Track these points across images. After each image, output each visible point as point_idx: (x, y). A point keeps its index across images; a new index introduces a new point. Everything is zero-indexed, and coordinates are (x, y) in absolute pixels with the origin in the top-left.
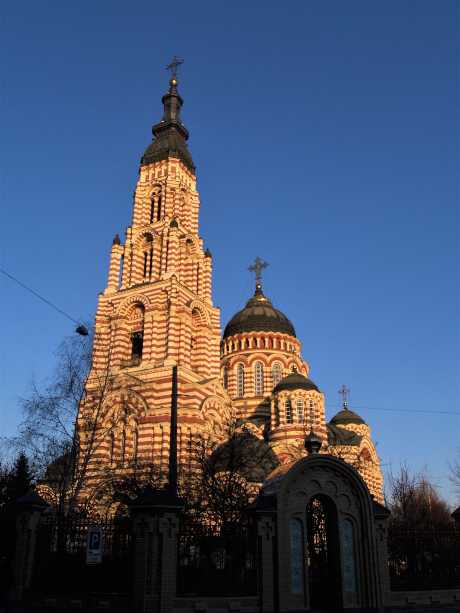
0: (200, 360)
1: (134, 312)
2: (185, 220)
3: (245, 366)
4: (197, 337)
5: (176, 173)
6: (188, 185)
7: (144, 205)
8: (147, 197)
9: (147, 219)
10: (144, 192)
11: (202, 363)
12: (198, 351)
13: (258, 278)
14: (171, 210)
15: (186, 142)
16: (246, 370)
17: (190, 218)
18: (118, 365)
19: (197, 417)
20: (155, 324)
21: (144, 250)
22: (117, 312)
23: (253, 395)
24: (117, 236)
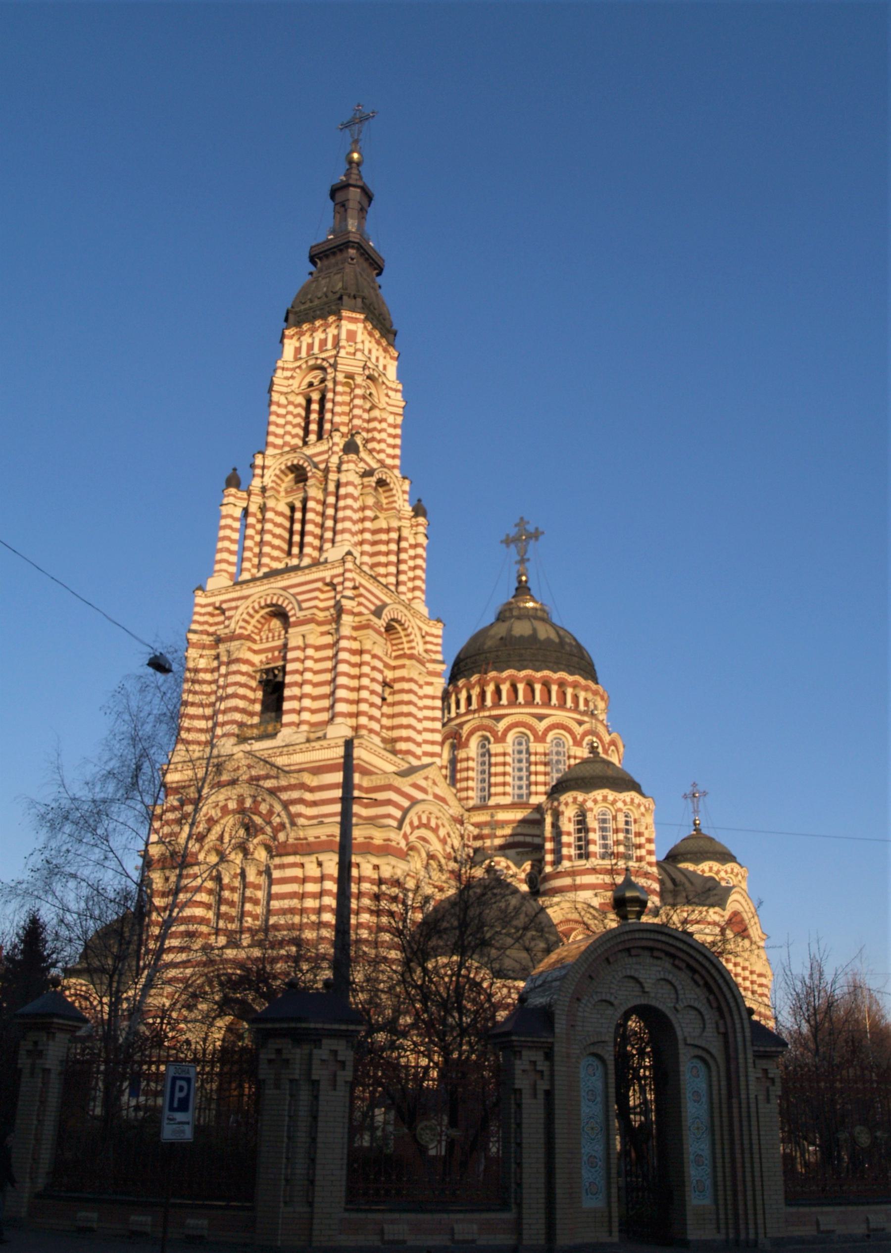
0: (401, 726)
1: (266, 627)
2: (373, 439)
3: (492, 739)
4: (395, 680)
5: (356, 343)
6: (381, 368)
7: (291, 408)
8: (297, 391)
9: (296, 436)
10: (291, 382)
11: (404, 733)
12: (397, 709)
13: (522, 561)
14: (345, 419)
15: (379, 279)
16: (495, 748)
17: (383, 435)
18: (233, 735)
19: (394, 844)
20: (310, 652)
21: (290, 500)
22: (233, 626)
23: (508, 800)
24: (235, 470)
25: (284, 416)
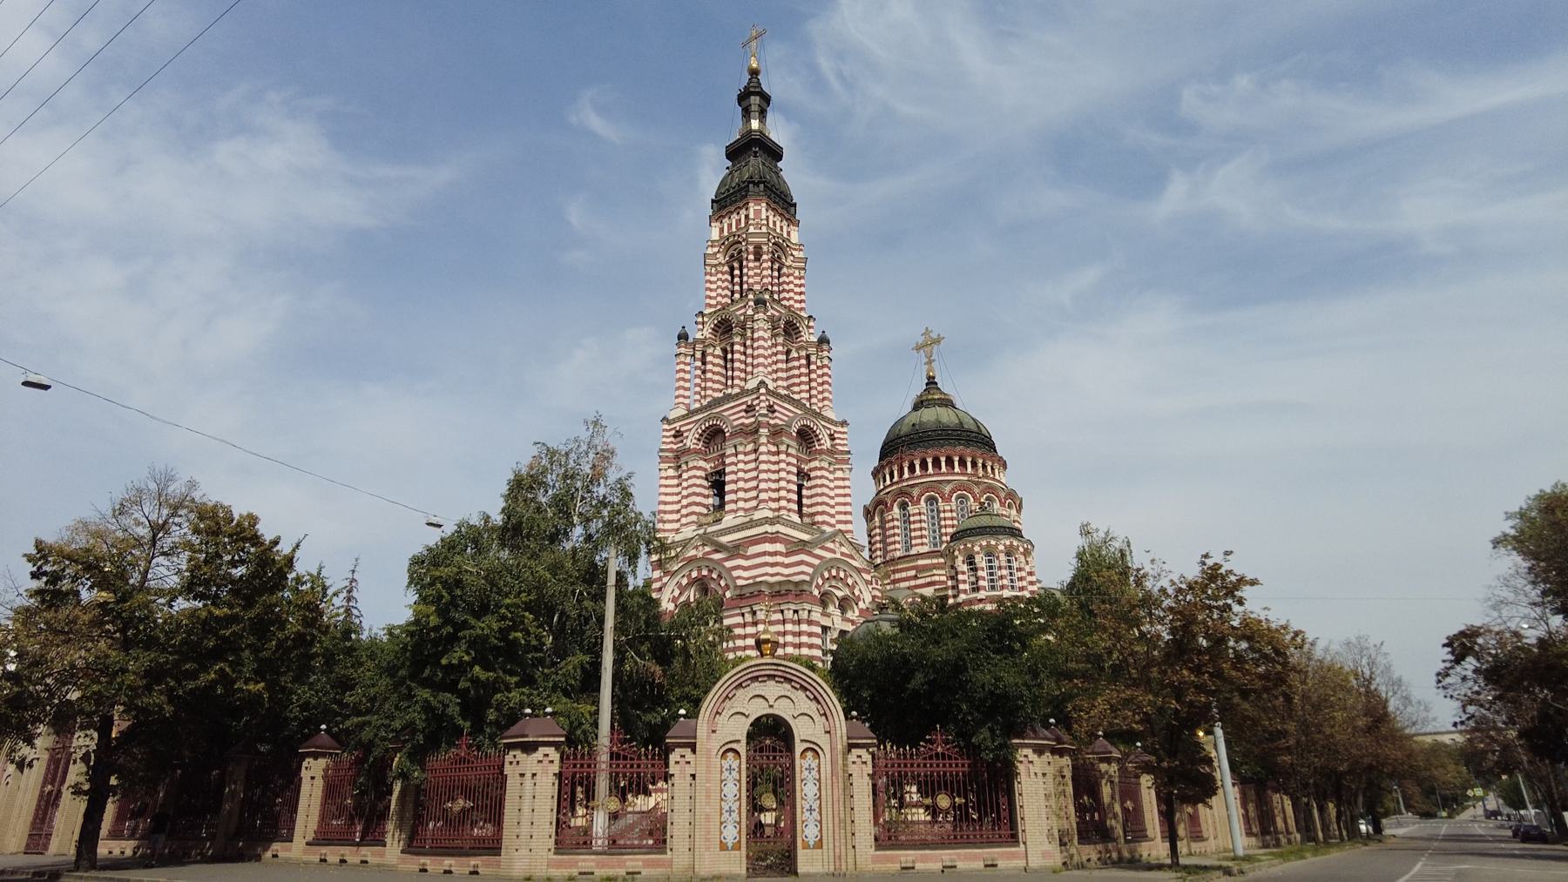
0: (817, 504)
2: (784, 290)
4: (810, 470)
6: (785, 235)
7: (720, 276)
9: (726, 296)
11: (820, 509)
12: (814, 491)
13: (930, 362)
14: (758, 279)
15: (779, 164)
17: (791, 286)
18: (693, 522)
20: (741, 457)
21: (723, 345)
22: (688, 444)
25: (715, 282)
